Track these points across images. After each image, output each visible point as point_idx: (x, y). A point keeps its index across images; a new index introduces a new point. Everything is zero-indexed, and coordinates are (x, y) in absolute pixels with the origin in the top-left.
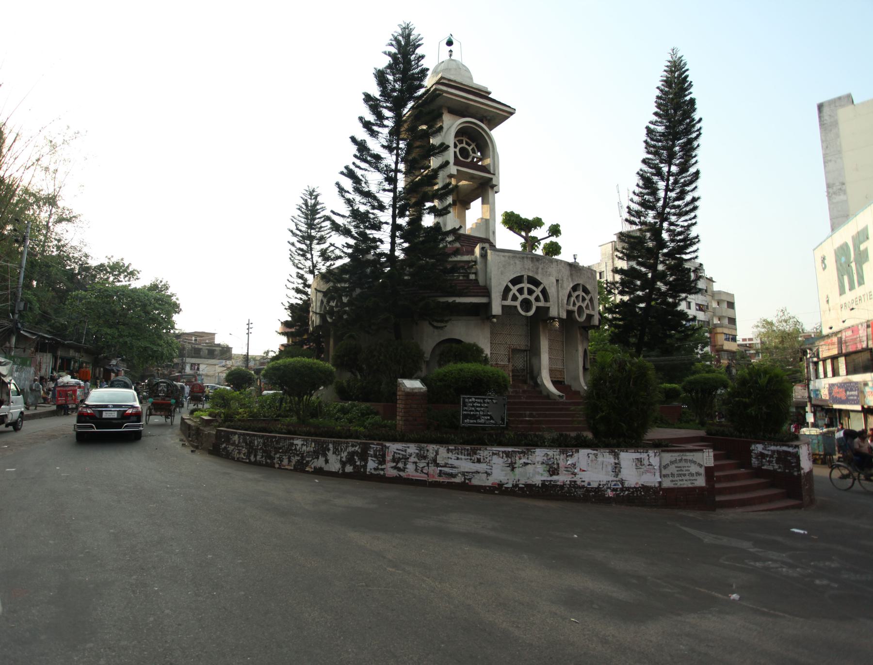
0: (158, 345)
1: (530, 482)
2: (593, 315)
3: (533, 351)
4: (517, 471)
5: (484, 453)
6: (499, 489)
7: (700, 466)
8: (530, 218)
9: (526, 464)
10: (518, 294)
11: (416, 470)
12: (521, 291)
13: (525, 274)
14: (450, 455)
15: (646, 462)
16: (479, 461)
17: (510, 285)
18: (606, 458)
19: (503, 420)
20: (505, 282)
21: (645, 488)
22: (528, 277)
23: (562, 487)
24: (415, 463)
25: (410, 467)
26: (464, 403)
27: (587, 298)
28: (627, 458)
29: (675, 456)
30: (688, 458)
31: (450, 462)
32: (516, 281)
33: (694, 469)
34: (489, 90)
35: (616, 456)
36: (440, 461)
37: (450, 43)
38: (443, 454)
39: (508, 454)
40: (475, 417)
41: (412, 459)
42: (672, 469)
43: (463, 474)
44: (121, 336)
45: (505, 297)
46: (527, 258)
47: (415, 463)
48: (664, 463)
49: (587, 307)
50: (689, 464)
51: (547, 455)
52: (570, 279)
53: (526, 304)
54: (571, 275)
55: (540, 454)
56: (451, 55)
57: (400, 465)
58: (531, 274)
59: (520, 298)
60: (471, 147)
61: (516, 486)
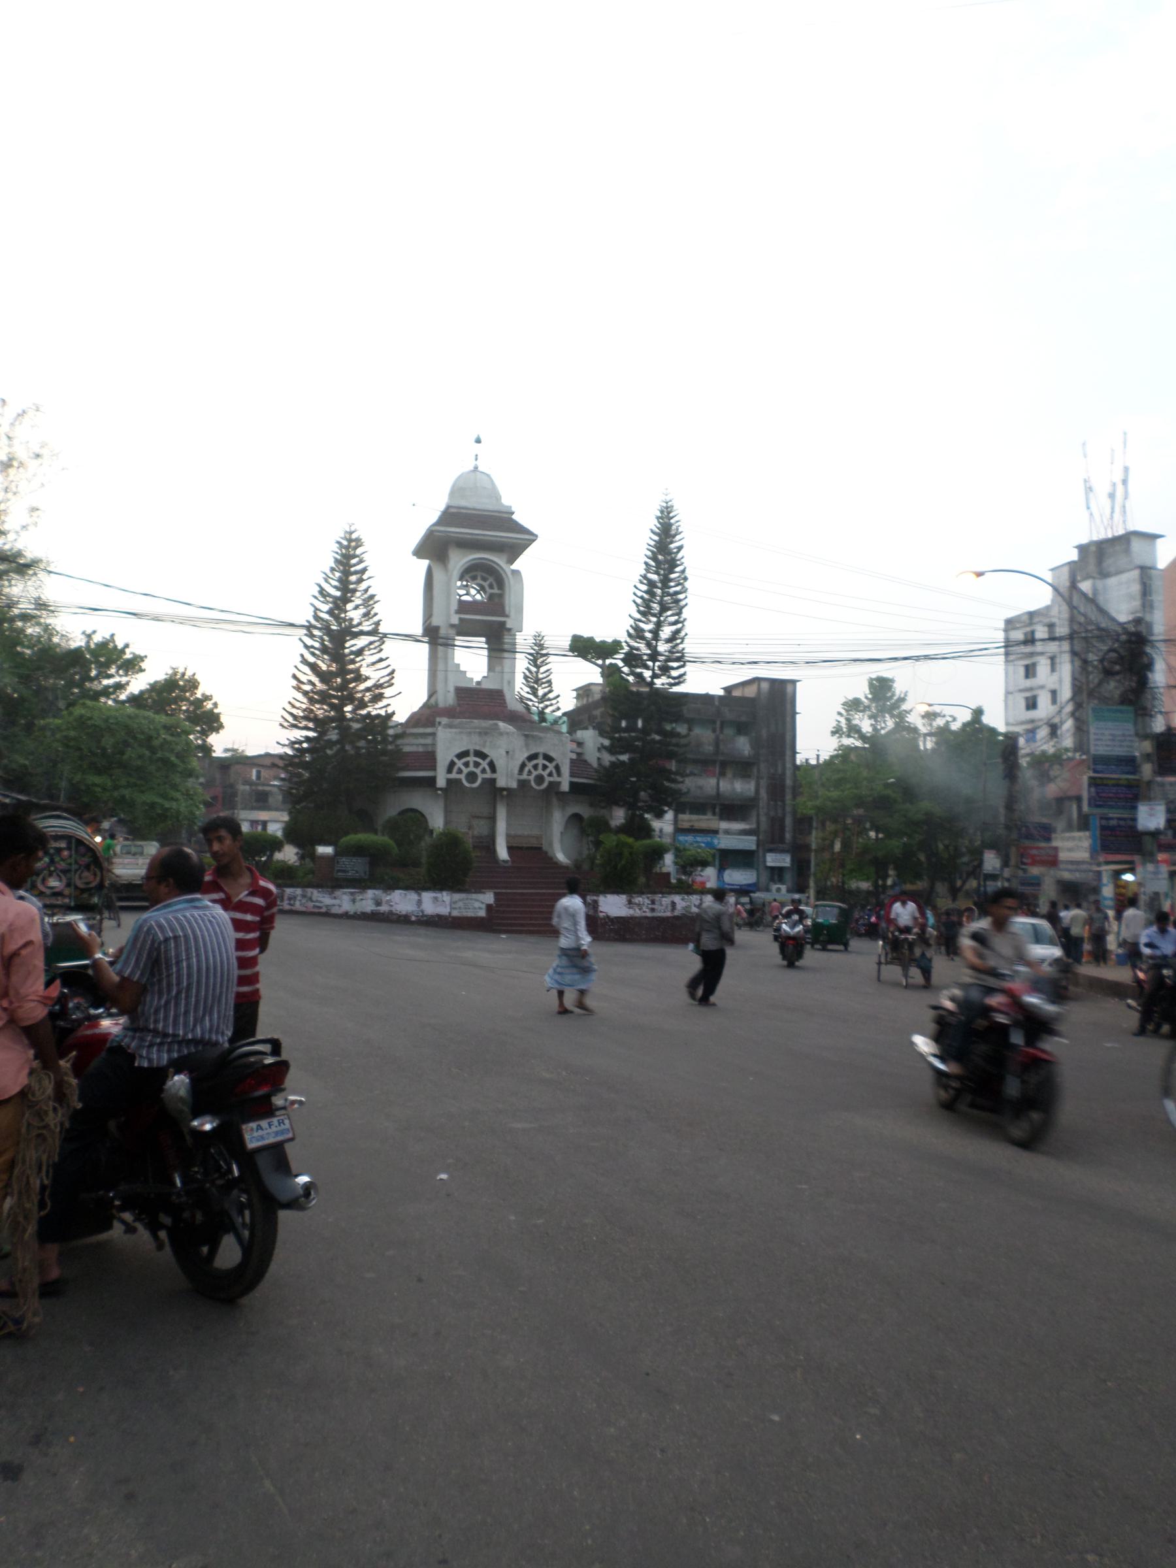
0: (172, 799)
1: (364, 911)
3: (492, 819)
4: (357, 904)
5: (338, 893)
6: (346, 916)
7: (483, 903)
8: (610, 640)
9: (362, 899)
10: (463, 768)
11: (301, 905)
13: (471, 748)
14: (319, 895)
15: (440, 899)
16: (335, 898)
18: (412, 896)
19: (365, 873)
21: (438, 916)
23: (383, 914)
24: (300, 900)
25: (298, 903)
26: (338, 862)
28: (427, 896)
29: (463, 896)
30: (473, 897)
31: (319, 899)
32: (461, 756)
33: (477, 905)
34: (513, 509)
35: (419, 895)
36: (314, 899)
37: (478, 441)
38: (315, 894)
39: (352, 894)
40: (344, 871)
41: (299, 898)
42: (460, 904)
43: (327, 906)
44: (116, 788)
45: (450, 769)
46: (475, 733)
47: (300, 900)
48: (454, 900)
49: (550, 775)
50: (474, 902)
51: (375, 894)
52: (524, 749)
54: (527, 745)
55: (370, 893)
57: (292, 902)
58: (478, 748)
59: (465, 771)
60: (488, 582)
61: (355, 913)
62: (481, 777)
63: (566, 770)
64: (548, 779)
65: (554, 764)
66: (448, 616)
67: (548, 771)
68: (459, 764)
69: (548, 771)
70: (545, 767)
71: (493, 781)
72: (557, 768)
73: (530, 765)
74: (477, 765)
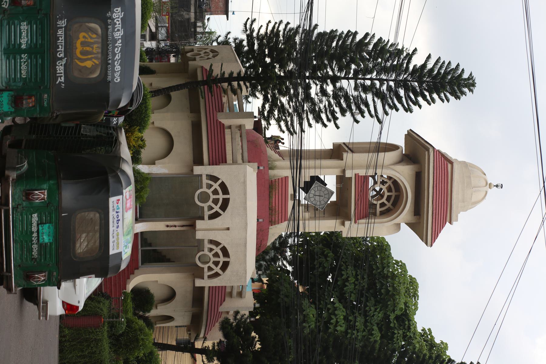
2: (203, 279)
12: (215, 192)
13: (231, 196)
17: (220, 182)
20: (223, 178)
27: (217, 269)
32: (223, 187)
34: (454, 223)
49: (210, 269)
53: (204, 198)
56: (497, 186)
59: (210, 191)
60: (386, 202)
62: (205, 206)
63: (216, 282)
64: (206, 267)
65: (220, 272)
66: (352, 168)
67: (213, 266)
68: (216, 186)
69: (213, 266)
70: (216, 263)
71: (202, 218)
72: (217, 275)
73: (217, 250)
74: (216, 201)
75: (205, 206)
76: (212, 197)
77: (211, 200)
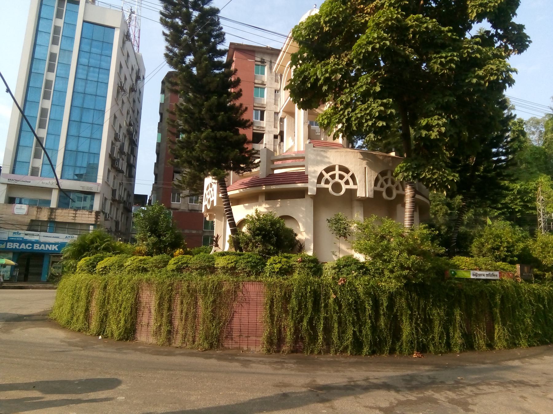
17: (324, 173)
22: (339, 166)
45: (319, 181)
59: (332, 182)
62: (344, 187)
68: (327, 176)
74: (341, 177)
75: (344, 187)
76: (337, 179)
77: (340, 181)
